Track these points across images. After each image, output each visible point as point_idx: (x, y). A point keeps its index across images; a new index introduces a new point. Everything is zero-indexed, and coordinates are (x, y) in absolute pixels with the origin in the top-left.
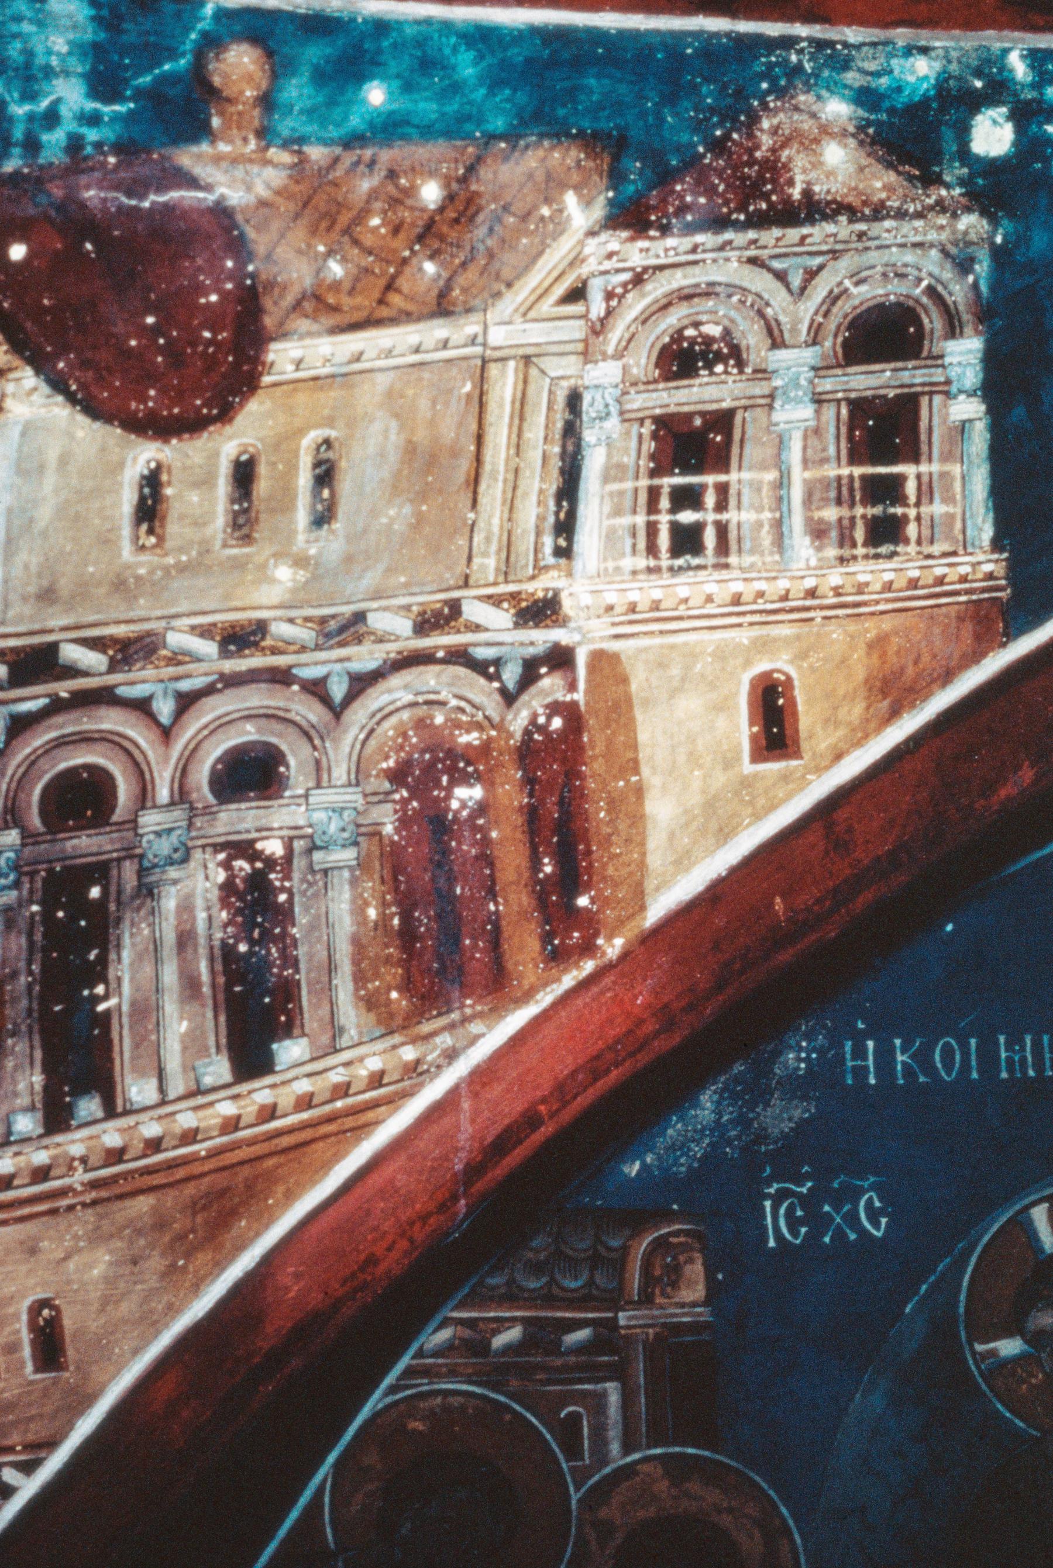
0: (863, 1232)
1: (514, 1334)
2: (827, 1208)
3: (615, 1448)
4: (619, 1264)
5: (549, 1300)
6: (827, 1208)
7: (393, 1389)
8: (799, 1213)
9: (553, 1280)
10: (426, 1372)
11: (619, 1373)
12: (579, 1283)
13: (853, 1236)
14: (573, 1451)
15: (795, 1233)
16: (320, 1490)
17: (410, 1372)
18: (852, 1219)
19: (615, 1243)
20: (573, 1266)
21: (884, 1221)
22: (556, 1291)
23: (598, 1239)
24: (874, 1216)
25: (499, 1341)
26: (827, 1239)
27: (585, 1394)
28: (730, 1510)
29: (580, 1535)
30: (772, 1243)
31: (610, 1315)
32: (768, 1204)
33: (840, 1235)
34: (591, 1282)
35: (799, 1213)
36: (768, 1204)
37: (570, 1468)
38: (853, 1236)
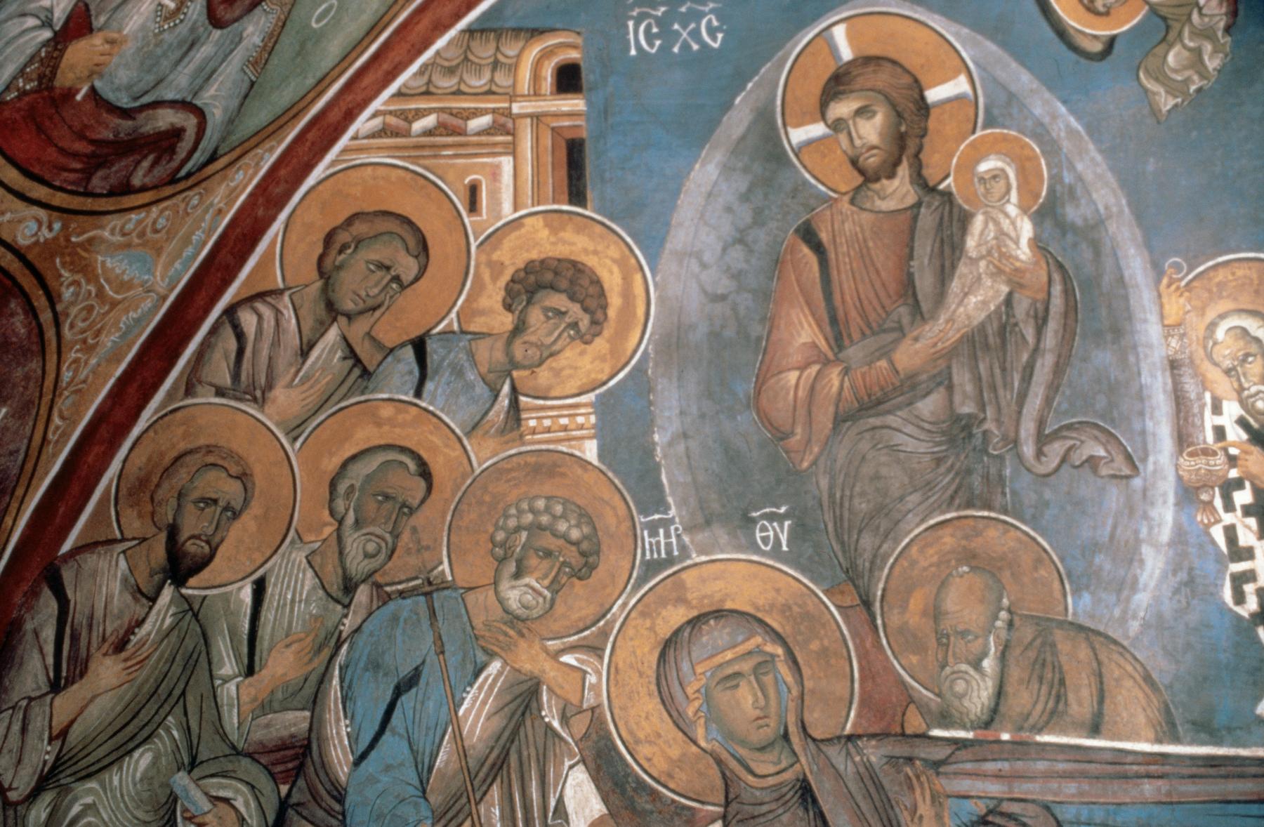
0: (704, 45)
1: (429, 121)
2: (676, 27)
3: (507, 206)
4: (513, 68)
5: (458, 93)
6: (676, 27)
7: (333, 163)
8: (655, 30)
9: (461, 80)
10: (360, 150)
11: (512, 150)
12: (482, 82)
13: (695, 47)
14: (473, 206)
15: (651, 45)
16: (273, 243)
17: (345, 151)
18: (696, 34)
19: (511, 53)
20: (479, 69)
21: (720, 36)
22: (463, 88)
23: (498, 48)
24: (712, 32)
25: (418, 126)
26: (676, 50)
27: (484, 165)
28: (595, 252)
29: (477, 275)
30: (633, 52)
31: (506, 105)
32: (631, 24)
33: (686, 47)
34: (492, 80)
35: (655, 30)
36: (631, 24)
37: (471, 222)
38: (695, 47)
